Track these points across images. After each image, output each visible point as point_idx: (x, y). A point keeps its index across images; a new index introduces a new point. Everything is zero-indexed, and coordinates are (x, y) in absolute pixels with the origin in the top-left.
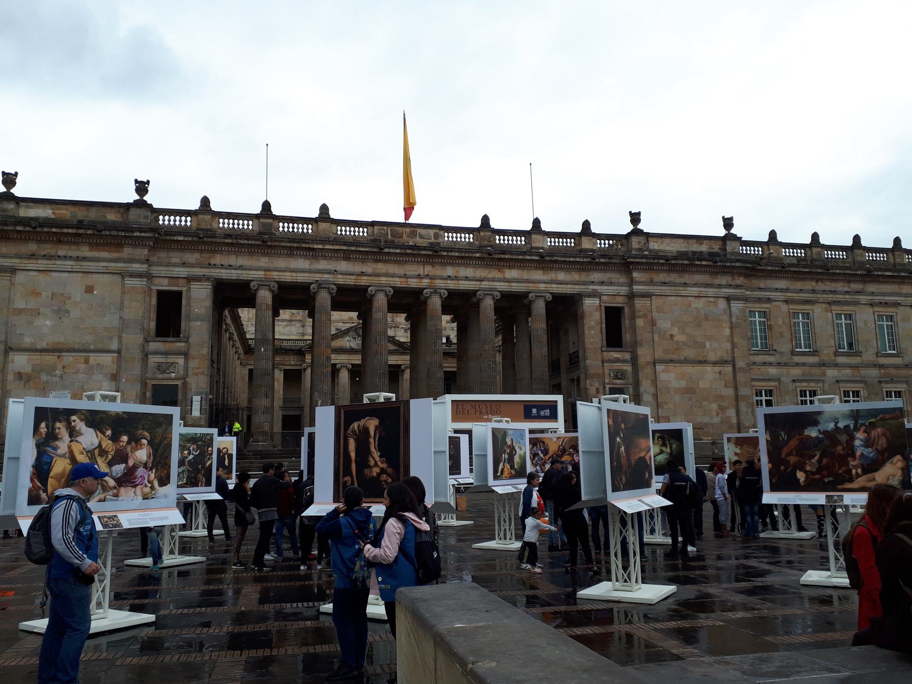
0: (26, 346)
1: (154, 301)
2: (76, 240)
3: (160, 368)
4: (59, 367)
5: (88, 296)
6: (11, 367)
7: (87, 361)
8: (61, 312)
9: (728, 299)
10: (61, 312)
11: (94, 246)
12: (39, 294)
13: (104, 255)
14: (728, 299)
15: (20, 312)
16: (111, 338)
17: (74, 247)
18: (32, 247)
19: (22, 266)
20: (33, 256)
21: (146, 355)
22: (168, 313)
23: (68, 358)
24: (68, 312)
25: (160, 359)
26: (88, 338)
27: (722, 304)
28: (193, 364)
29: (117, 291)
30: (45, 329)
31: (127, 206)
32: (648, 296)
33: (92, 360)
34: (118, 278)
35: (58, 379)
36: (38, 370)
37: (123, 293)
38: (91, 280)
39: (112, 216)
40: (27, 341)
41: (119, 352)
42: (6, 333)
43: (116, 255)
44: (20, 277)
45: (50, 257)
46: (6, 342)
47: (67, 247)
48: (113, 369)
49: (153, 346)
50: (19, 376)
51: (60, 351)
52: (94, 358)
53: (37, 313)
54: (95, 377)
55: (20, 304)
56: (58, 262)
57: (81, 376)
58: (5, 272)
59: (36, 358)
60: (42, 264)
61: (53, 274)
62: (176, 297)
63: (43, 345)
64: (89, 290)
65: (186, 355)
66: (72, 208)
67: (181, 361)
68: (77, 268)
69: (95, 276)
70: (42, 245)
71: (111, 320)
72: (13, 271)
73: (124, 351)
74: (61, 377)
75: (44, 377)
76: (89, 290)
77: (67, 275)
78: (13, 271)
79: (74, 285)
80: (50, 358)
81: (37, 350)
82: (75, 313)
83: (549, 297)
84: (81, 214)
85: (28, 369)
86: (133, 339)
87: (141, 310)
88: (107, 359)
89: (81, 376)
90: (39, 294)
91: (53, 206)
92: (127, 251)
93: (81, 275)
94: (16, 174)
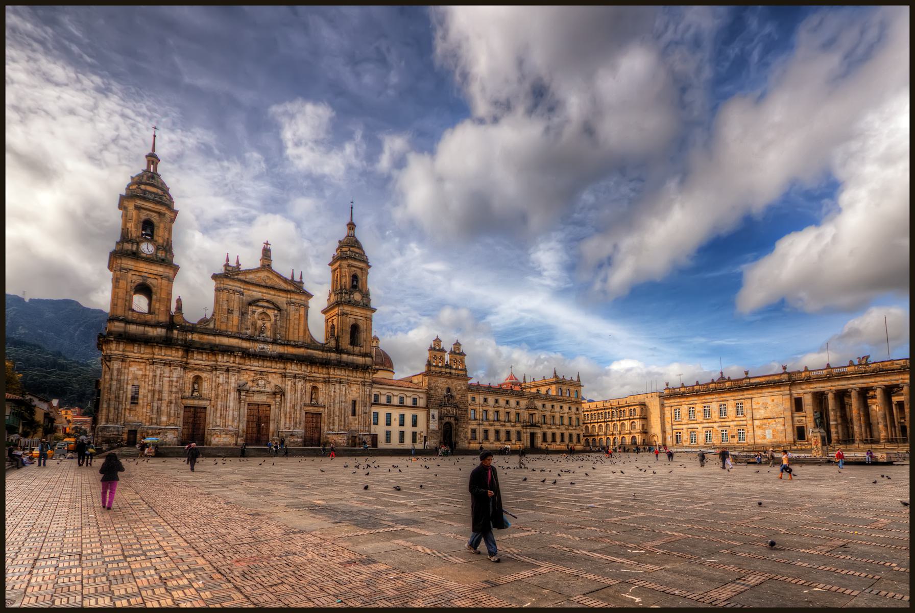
21: (793, 418)
23: (770, 421)
30: (761, 413)
40: (758, 417)
71: (780, 408)
80: (765, 421)
86: (788, 414)
87: (787, 405)
88: (781, 420)
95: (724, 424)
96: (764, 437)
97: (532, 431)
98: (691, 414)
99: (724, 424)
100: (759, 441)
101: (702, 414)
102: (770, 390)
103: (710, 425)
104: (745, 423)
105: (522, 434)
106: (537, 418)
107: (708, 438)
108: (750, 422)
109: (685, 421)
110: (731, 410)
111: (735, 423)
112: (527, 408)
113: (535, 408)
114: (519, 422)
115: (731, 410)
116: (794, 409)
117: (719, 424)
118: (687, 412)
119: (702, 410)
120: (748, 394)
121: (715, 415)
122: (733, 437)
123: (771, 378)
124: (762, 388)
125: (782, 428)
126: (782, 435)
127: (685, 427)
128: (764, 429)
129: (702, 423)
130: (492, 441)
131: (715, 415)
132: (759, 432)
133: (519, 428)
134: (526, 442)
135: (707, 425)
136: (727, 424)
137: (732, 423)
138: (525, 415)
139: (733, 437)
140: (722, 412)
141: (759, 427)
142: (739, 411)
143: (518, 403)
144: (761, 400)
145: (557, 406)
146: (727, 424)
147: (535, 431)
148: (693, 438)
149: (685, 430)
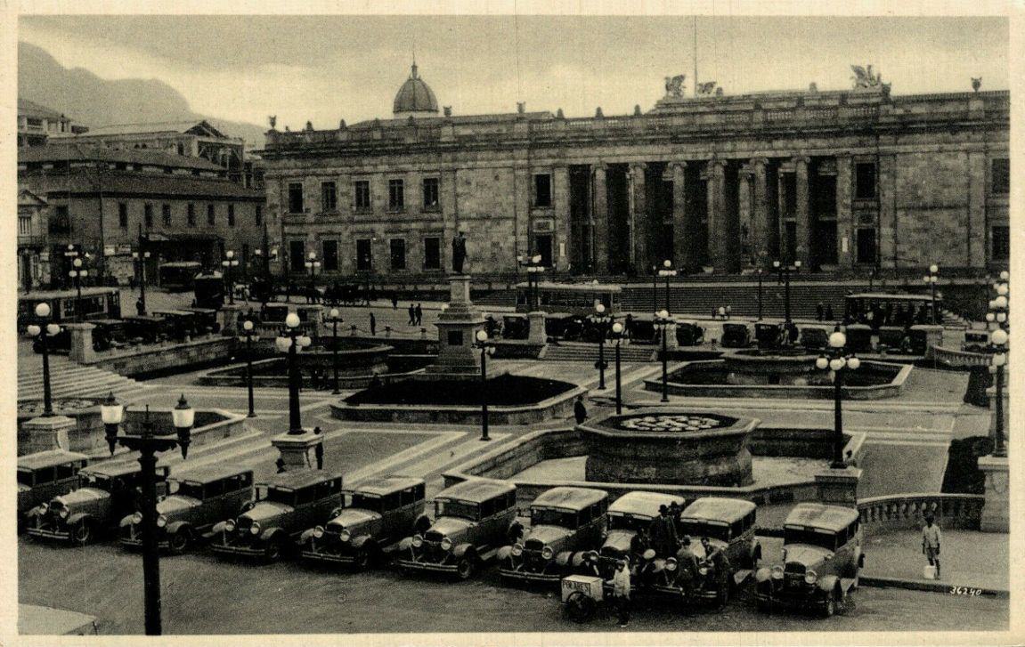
1: (534, 183)
3: (540, 226)
9: (967, 152)
14: (967, 152)
21: (531, 218)
22: (542, 188)
25: (541, 221)
27: (962, 156)
28: (559, 222)
32: (894, 155)
46: (456, 214)
49: (537, 213)
62: (547, 178)
65: (554, 218)
67: (551, 221)
83: (808, 160)
103: (367, 227)
108: (450, 225)
111: (420, 225)
116: (534, 199)
129: (352, 221)
135: (360, 227)
136: (404, 226)
137: (414, 225)
149: (312, 237)
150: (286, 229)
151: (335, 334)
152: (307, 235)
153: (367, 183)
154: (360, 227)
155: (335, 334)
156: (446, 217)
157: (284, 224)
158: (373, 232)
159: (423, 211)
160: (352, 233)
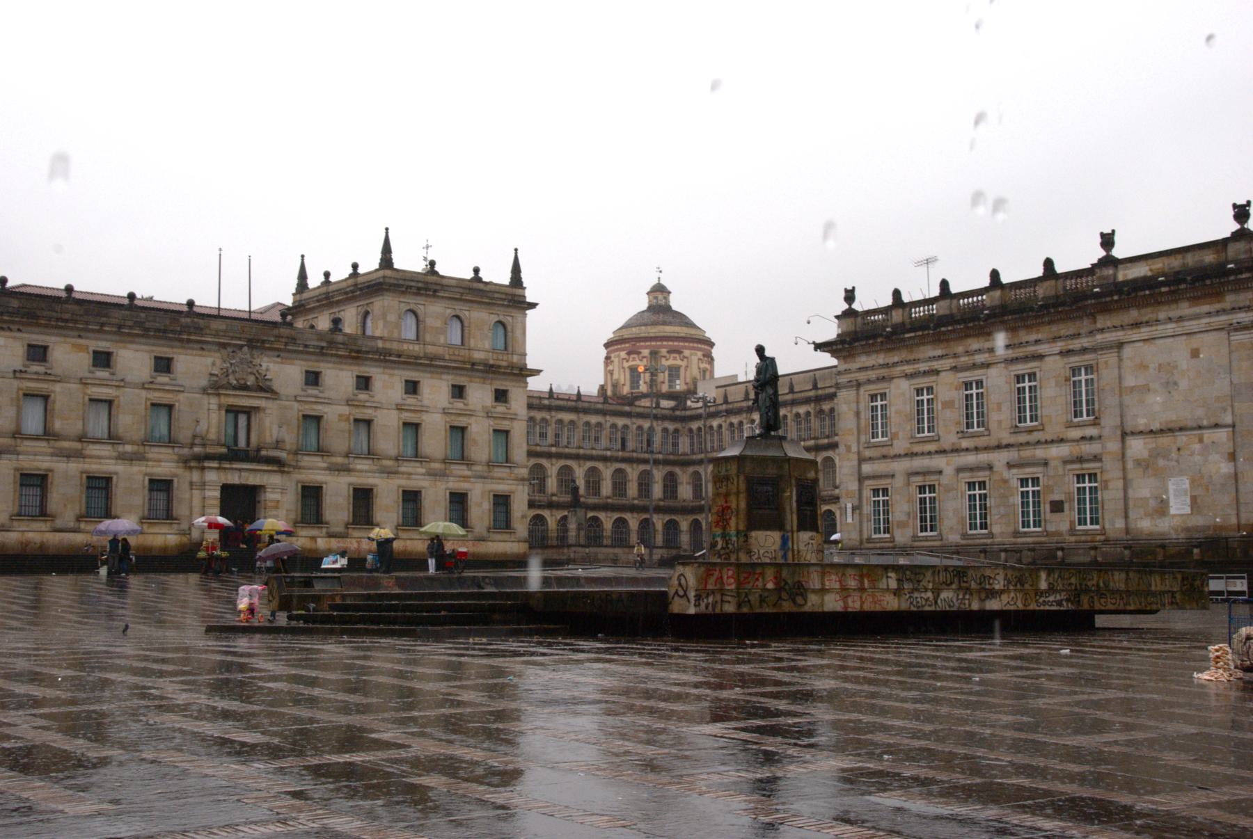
0: (1141, 428)
2: (1174, 298)
4: (1174, 449)
5: (1194, 361)
6: (1129, 453)
7: (1201, 441)
8: (1170, 385)
10: (1170, 385)
11: (1195, 300)
12: (1146, 367)
13: (1206, 308)
15: (1132, 389)
16: (1225, 410)
17: (1174, 306)
18: (1134, 314)
19: (1127, 338)
20: (1136, 325)
23: (1182, 438)
24: (1175, 383)
26: (1200, 412)
29: (1225, 351)
30: (1154, 408)
31: (1219, 245)
33: (1205, 437)
34: (1223, 334)
35: (1174, 463)
36: (1156, 454)
37: (1230, 353)
38: (1196, 341)
39: (1209, 258)
40: (1142, 423)
41: (1234, 426)
42: (1122, 416)
43: (1218, 306)
44: (1128, 351)
45: (1147, 323)
47: (1166, 307)
48: (1228, 447)
50: (1138, 463)
51: (1171, 430)
52: (1208, 435)
53: (1146, 389)
54: (1210, 458)
55: (1130, 381)
56: (1160, 327)
57: (1197, 458)
58: (1111, 348)
59: (1151, 442)
60: (1145, 332)
61: (1161, 341)
63: (1156, 426)
64: (1195, 354)
66: (1166, 260)
68: (1179, 331)
69: (1198, 336)
70: (1143, 311)
71: (1222, 386)
72: (1120, 345)
73: (1238, 424)
74: (1177, 461)
75: (1161, 462)
76: (1195, 354)
77: (1171, 340)
78: (1120, 345)
79: (1178, 351)
80: (1164, 440)
81: (1151, 432)
82: (1184, 384)
84: (1176, 263)
85: (1145, 454)
88: (1222, 435)
89: (1197, 458)
90: (1146, 367)
91: (1150, 262)
92: (1230, 300)
93: (1184, 337)
94: (1113, 231)
95: (1027, 453)
96: (1162, 509)
97: (234, 479)
98: (923, 414)
99: (1027, 453)
100: (1145, 525)
101: (957, 414)
102: (1185, 309)
103: (983, 457)
104: (1094, 448)
105: (181, 491)
106: (274, 425)
107: (980, 511)
108: (1113, 446)
109: (900, 446)
110: (1053, 399)
112: (216, 387)
113: (264, 388)
114: (171, 442)
115: (1053, 399)
117: (1012, 455)
118: (910, 408)
119: (958, 396)
120: (1108, 329)
121: (1001, 417)
122: (1057, 507)
123: (1190, 260)
124: (1157, 301)
125: (1226, 468)
126: (1227, 498)
127: (900, 466)
128: (1162, 476)
129: (956, 451)
130: (67, 517)
131: (1001, 417)
132: (1143, 489)
133: (164, 464)
134: (203, 517)
135: (971, 459)
136: (1040, 453)
138: (206, 419)
139: (1057, 507)
140: (1025, 402)
141: (1145, 465)
142: (1085, 407)
143: (163, 365)
144: (1153, 354)
145: (389, 386)
146: (1040, 453)
147: (253, 480)
148: (928, 517)
149: (899, 481)
150: (867, 468)
151: (814, 591)
152: (893, 476)
153: (979, 384)
154: (971, 459)
155: (814, 591)
156: (1106, 432)
157: (861, 460)
158: (990, 467)
159: (1070, 425)
160: (960, 470)
